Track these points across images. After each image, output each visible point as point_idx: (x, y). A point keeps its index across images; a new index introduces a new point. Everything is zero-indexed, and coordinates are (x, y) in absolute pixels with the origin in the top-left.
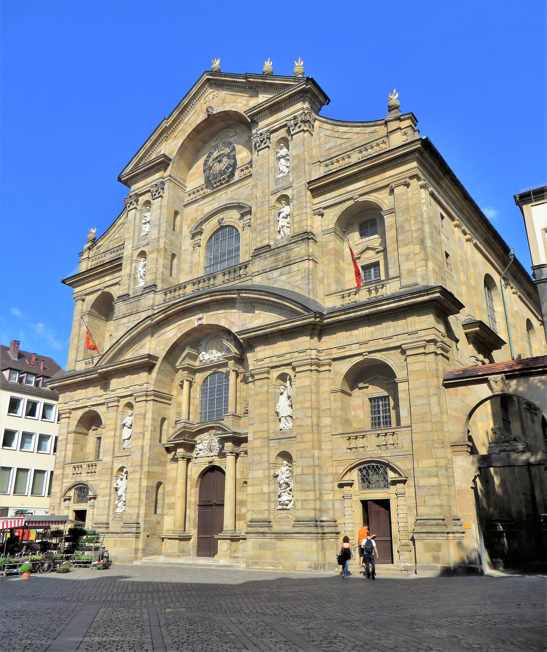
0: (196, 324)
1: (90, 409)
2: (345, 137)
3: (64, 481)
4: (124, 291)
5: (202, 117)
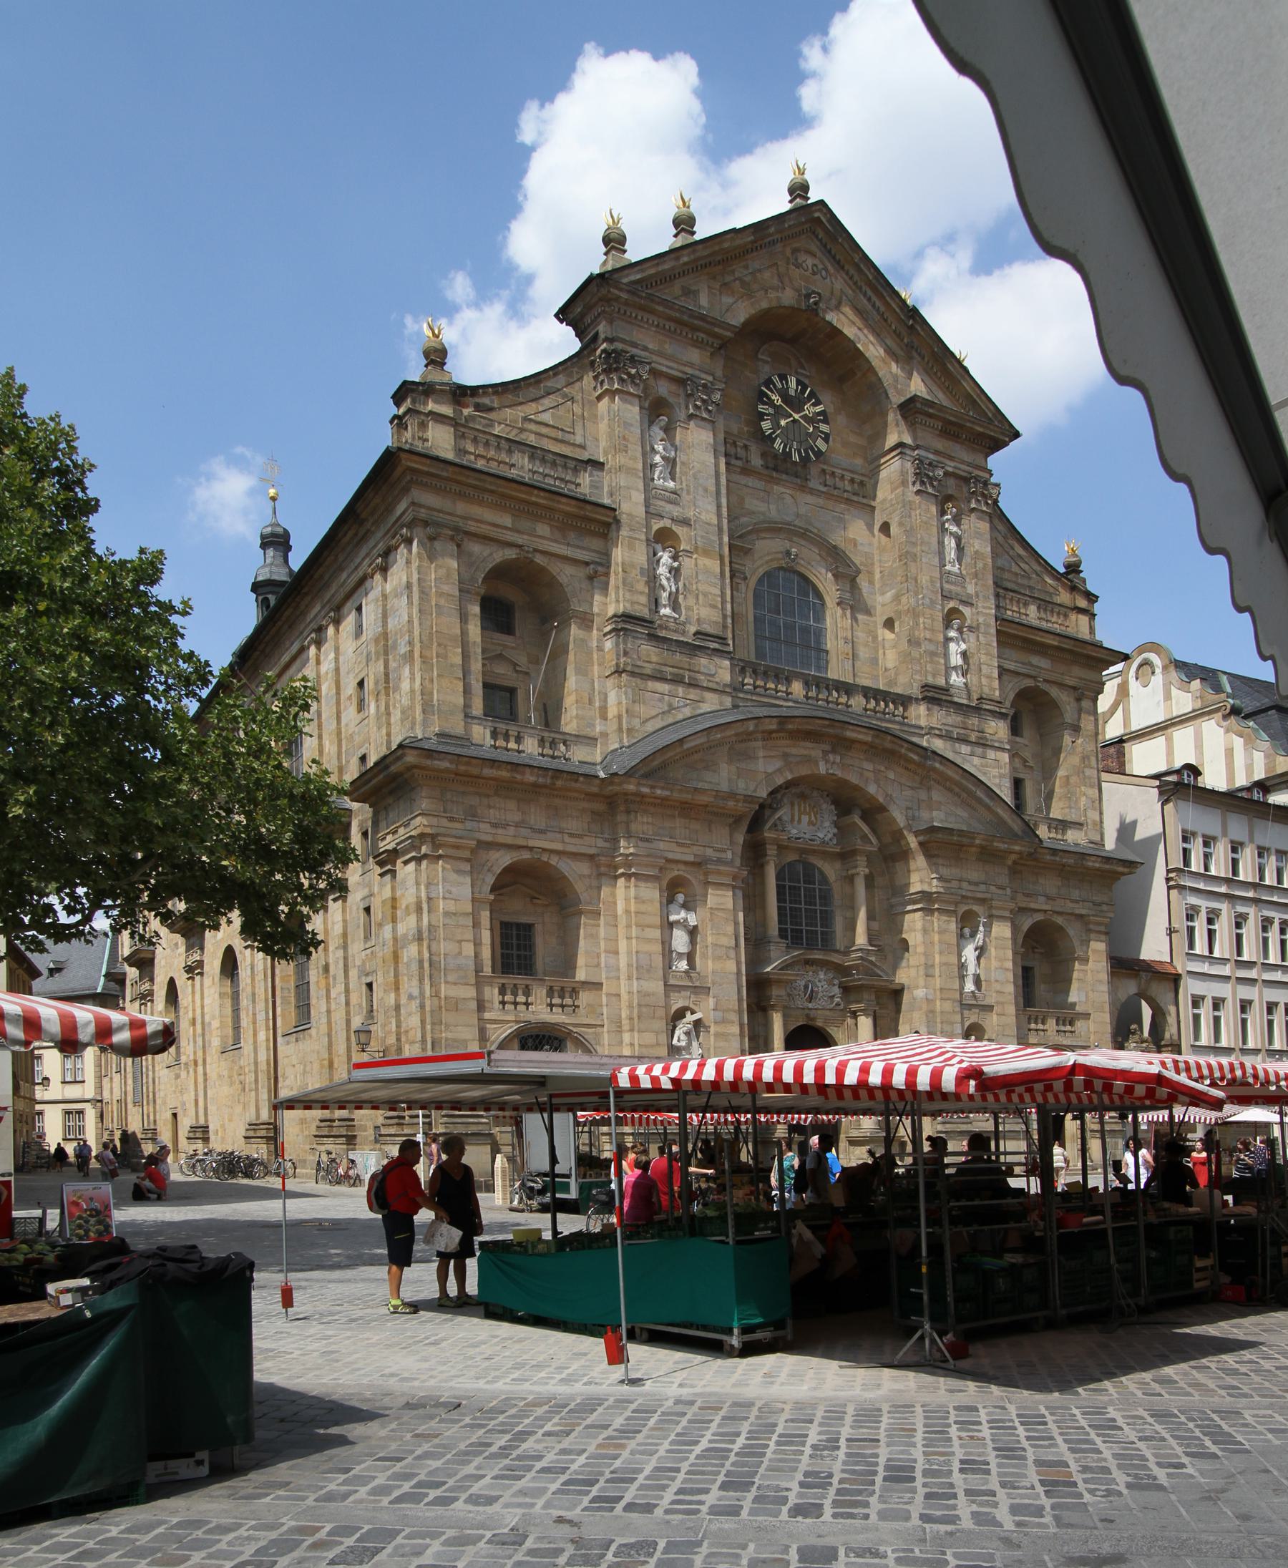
0: (822, 769)
2: (1022, 565)
4: (636, 607)
5: (788, 297)
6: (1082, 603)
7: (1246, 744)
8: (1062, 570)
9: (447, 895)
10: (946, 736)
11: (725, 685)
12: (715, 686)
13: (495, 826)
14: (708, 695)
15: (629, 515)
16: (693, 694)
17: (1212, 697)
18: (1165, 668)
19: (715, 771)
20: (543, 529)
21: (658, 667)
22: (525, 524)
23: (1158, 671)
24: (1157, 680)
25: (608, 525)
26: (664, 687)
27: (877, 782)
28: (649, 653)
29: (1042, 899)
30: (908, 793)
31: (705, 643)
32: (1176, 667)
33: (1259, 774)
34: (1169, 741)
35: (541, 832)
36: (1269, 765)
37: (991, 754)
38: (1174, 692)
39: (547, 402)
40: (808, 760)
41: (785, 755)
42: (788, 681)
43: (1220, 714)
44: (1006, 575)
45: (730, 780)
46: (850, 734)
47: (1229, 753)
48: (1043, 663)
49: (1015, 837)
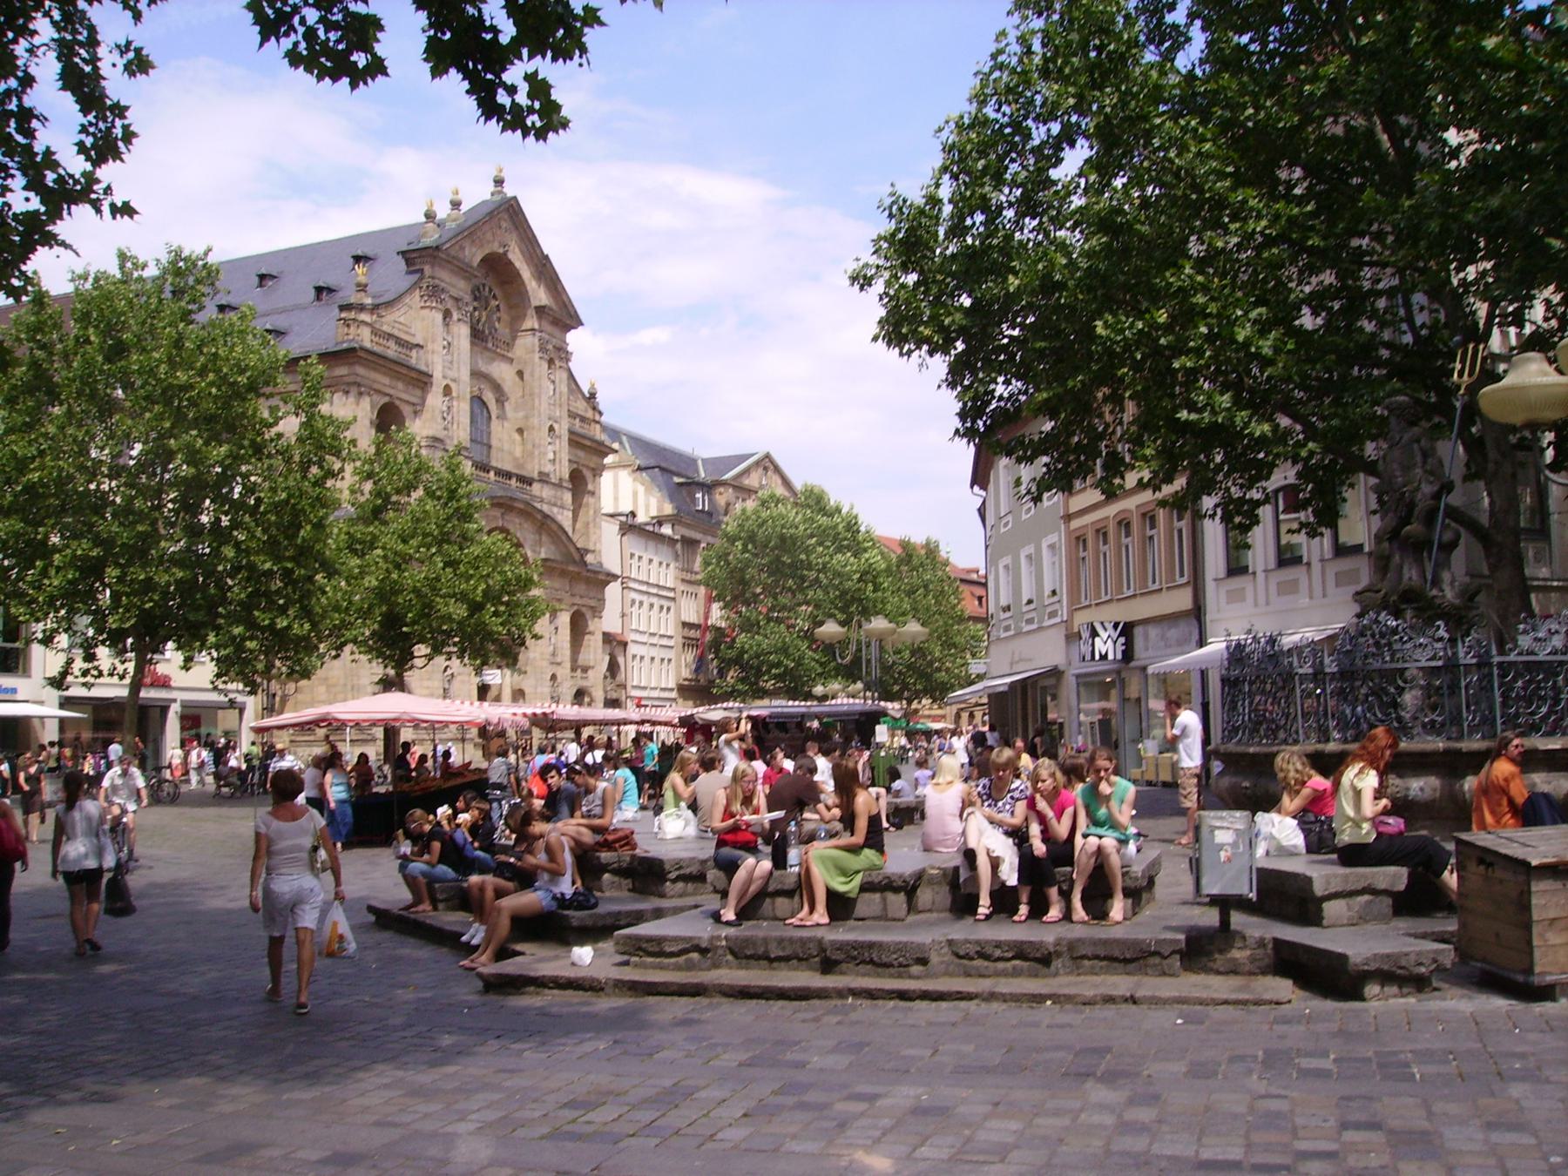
7: (646, 490)
20: (400, 385)
22: (394, 383)
25: (426, 383)
33: (654, 513)
36: (660, 509)
37: (565, 512)
39: (402, 311)
42: (488, 472)
43: (630, 469)
46: (516, 505)
47: (635, 494)
48: (581, 454)
49: (574, 562)
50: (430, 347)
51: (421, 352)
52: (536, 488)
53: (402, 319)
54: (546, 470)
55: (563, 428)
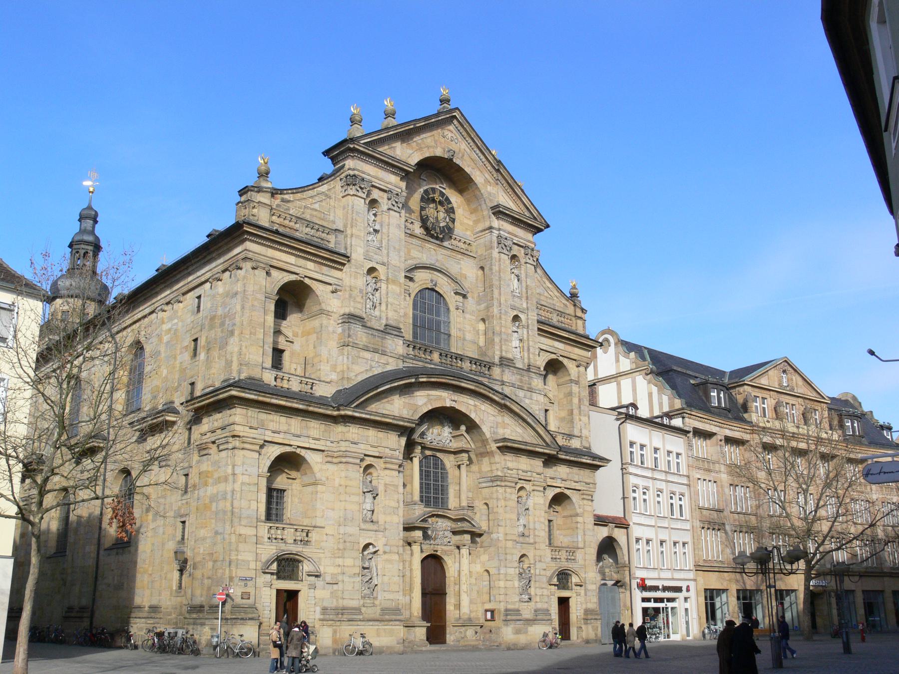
0: (448, 404)
1: (294, 450)
3: (259, 546)
6: (579, 314)
7: (659, 391)
8: (569, 295)
9: (245, 473)
10: (513, 385)
11: (400, 355)
12: (394, 356)
13: (274, 432)
14: (391, 360)
15: (356, 260)
16: (384, 359)
17: (641, 363)
18: (616, 344)
19: (392, 404)
21: (366, 344)
23: (613, 345)
24: (612, 349)
26: (368, 355)
27: (475, 411)
28: (360, 335)
29: (559, 481)
30: (492, 418)
31: (391, 330)
32: (622, 344)
33: (666, 409)
34: (619, 385)
35: (298, 436)
36: (671, 404)
38: (621, 358)
40: (440, 398)
41: (428, 395)
44: (542, 298)
45: (399, 409)
47: (650, 395)
50: (349, 232)
51: (341, 237)
52: (496, 372)
53: (316, 206)
54: (510, 356)
55: (530, 318)
